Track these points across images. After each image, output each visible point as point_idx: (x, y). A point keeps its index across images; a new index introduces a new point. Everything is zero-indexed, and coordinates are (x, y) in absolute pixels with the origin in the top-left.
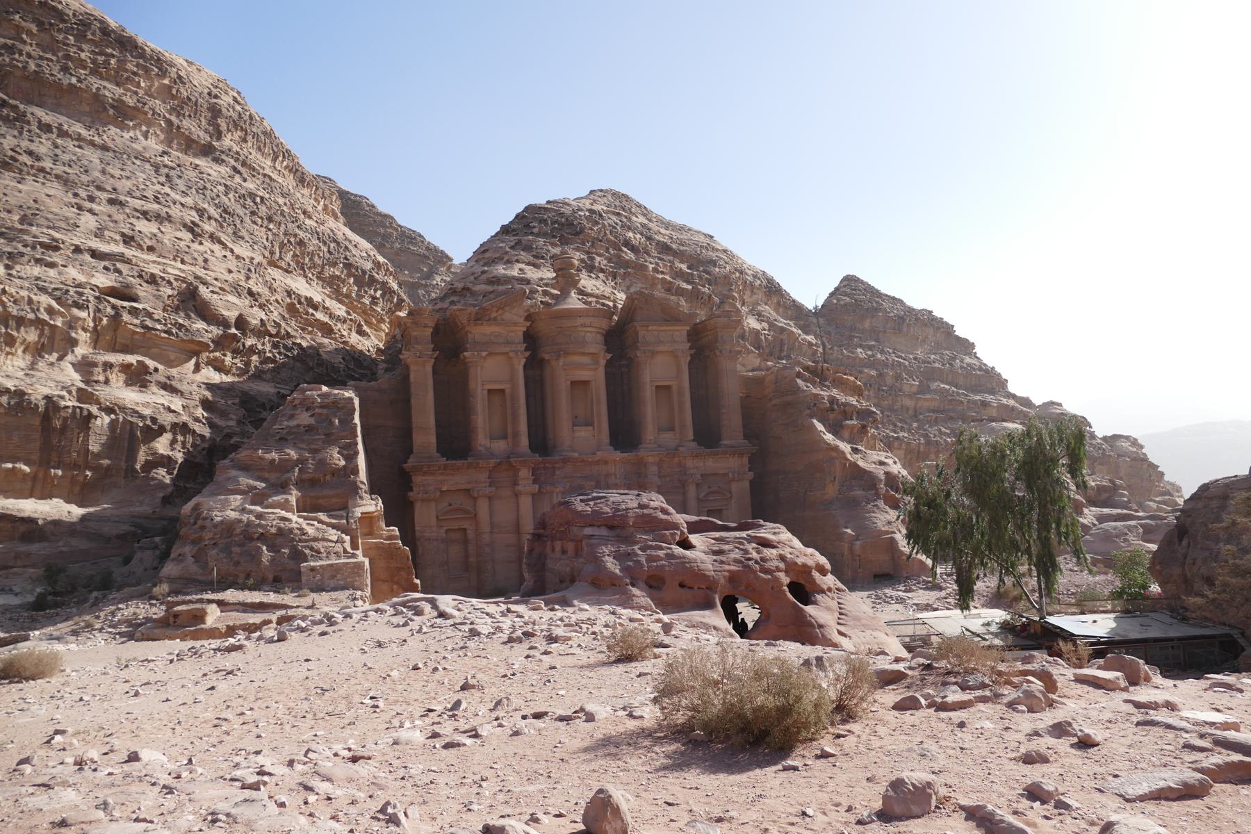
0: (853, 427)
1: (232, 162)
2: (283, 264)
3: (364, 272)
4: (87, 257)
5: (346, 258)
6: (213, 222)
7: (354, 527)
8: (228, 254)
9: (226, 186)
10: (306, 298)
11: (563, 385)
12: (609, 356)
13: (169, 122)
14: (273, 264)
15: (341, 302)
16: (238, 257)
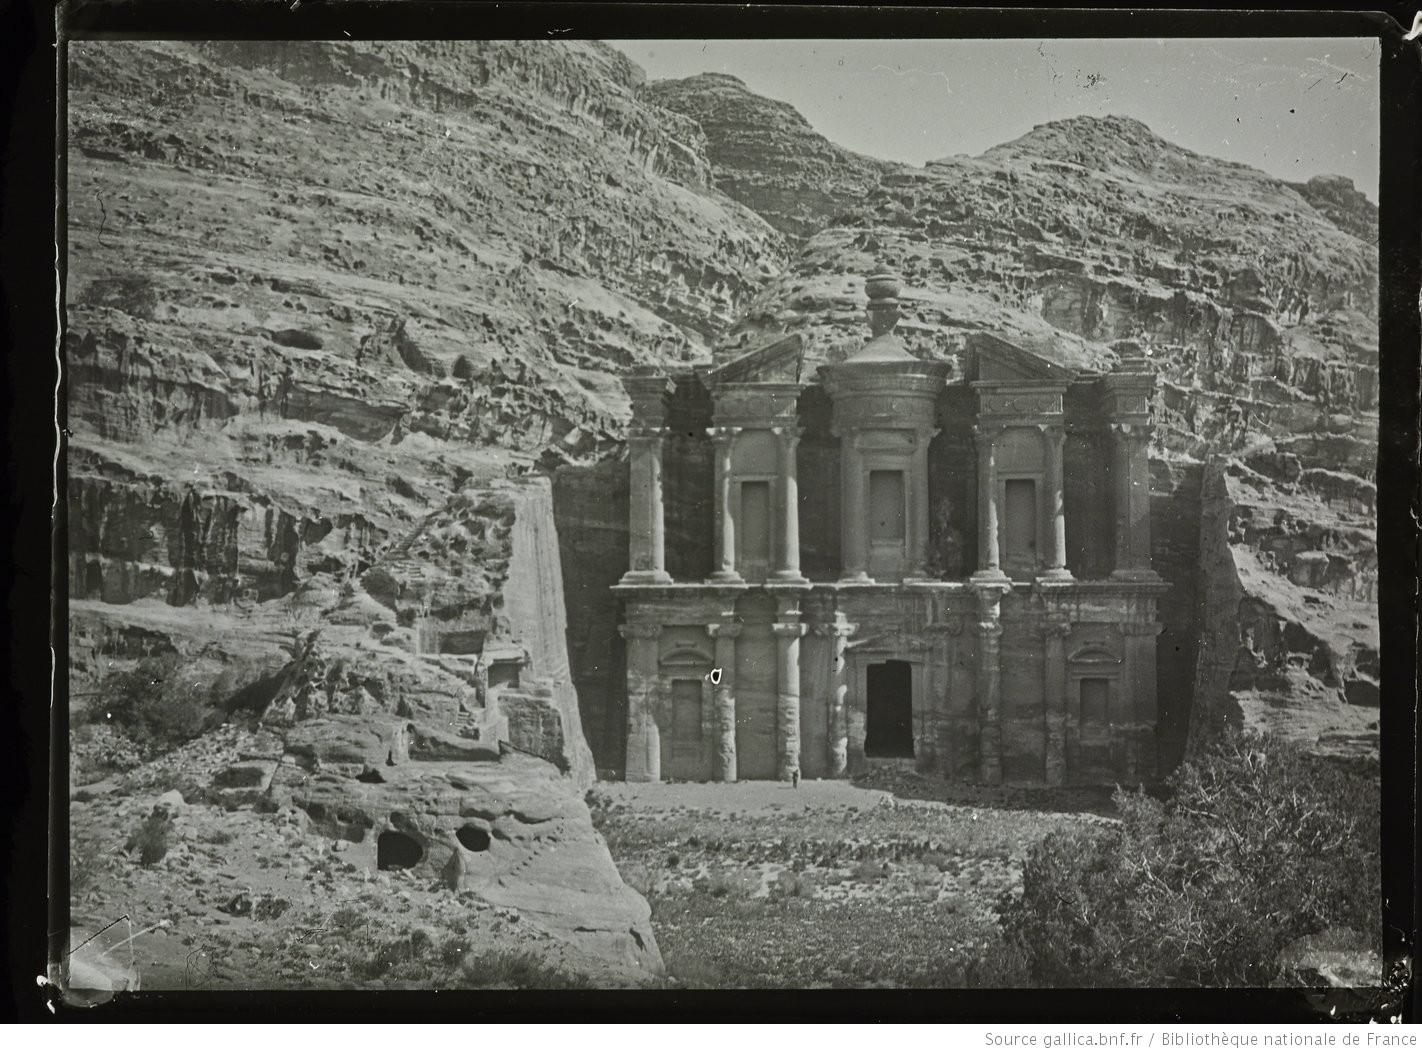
0: (1315, 565)
1: (501, 115)
2: (564, 264)
3: (699, 262)
4: (268, 289)
5: (670, 244)
6: (457, 214)
7: (481, 678)
8: (469, 262)
9: (482, 154)
10: (593, 314)
11: (858, 476)
12: (935, 433)
13: (414, 69)
14: (547, 265)
15: (660, 312)
16: (484, 265)
